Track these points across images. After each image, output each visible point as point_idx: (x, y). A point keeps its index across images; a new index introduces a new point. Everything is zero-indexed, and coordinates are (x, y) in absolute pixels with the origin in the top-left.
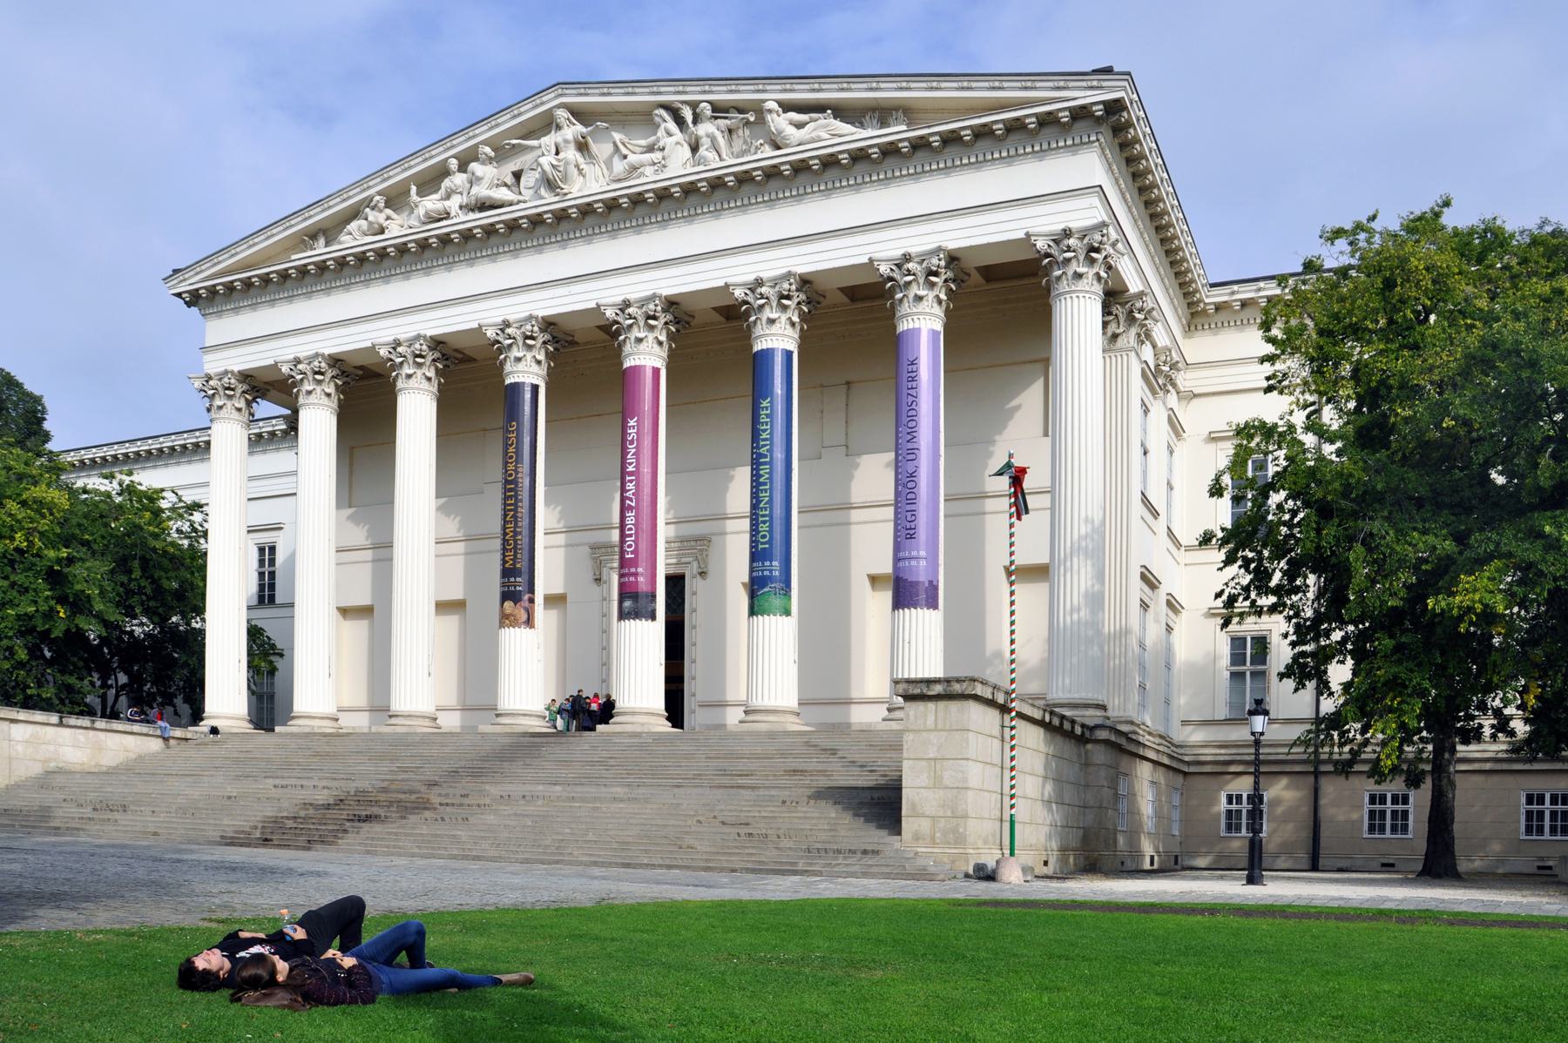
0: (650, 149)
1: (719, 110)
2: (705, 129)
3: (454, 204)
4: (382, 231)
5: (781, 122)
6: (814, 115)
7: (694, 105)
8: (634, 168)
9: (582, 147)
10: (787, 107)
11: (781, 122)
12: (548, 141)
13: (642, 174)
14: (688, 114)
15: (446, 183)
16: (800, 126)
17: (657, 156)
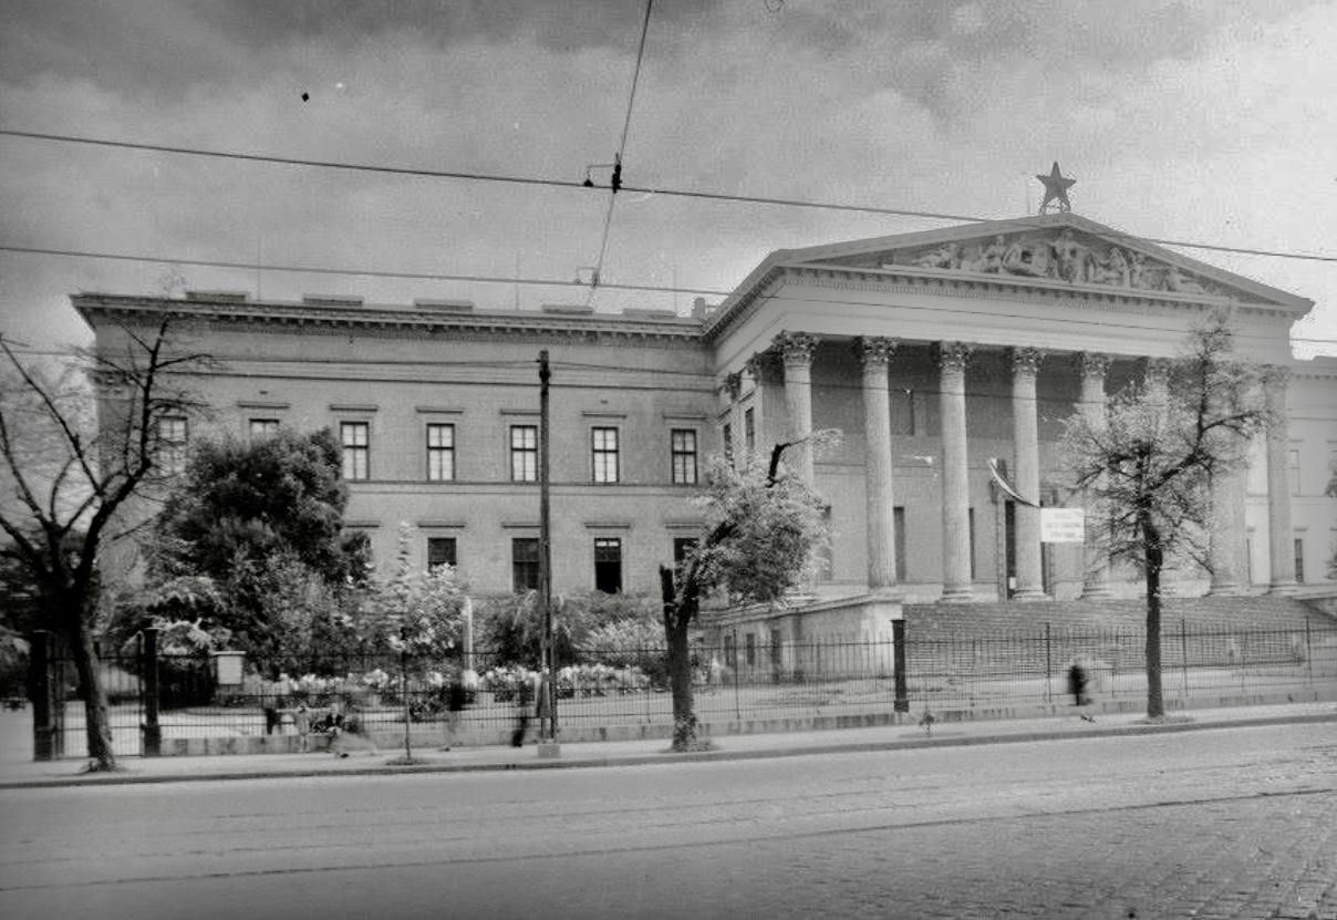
0: (1108, 267)
1: (1148, 258)
2: (1139, 268)
3: (997, 262)
4: (946, 265)
5: (1177, 278)
6: (1189, 279)
7: (1136, 253)
8: (1107, 279)
9: (1073, 252)
10: (1181, 271)
11: (1177, 278)
12: (1058, 244)
13: (1110, 284)
14: (1134, 257)
15: (992, 249)
16: (1183, 282)
17: (1113, 274)
